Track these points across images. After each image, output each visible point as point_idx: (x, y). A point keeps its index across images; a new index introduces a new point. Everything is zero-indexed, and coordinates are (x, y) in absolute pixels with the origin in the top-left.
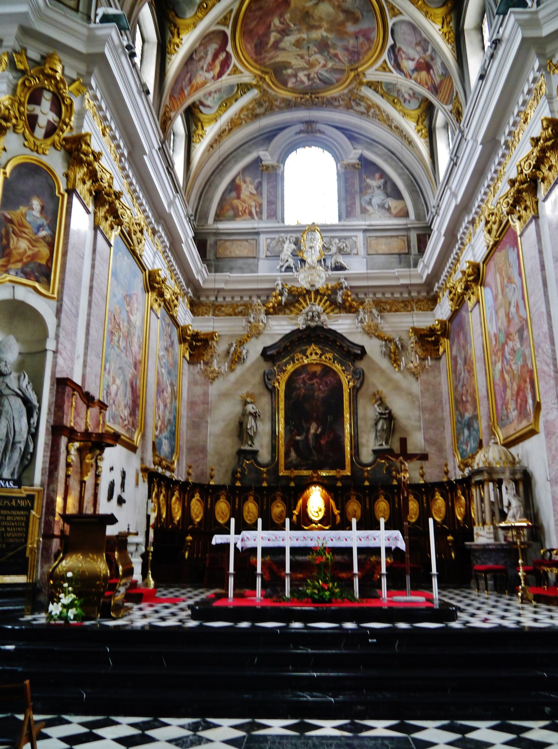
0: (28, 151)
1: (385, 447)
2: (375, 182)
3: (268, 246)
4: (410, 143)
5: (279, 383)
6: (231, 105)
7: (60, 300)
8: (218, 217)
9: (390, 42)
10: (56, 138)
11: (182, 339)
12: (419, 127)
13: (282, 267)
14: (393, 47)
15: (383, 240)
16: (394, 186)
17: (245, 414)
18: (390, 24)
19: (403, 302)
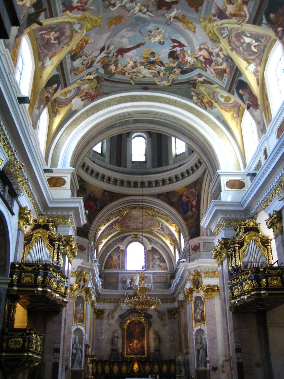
0: (79, 293)
1: (157, 348)
2: (156, 257)
3: (122, 278)
4: (168, 246)
5: (125, 326)
6: (112, 234)
7: (85, 326)
8: (106, 268)
9: (161, 227)
10: (84, 288)
11: (95, 312)
12: (171, 242)
13: (126, 287)
14: (162, 228)
15: (159, 278)
16: (163, 258)
17: (114, 337)
18: (161, 224)
19: (165, 299)
